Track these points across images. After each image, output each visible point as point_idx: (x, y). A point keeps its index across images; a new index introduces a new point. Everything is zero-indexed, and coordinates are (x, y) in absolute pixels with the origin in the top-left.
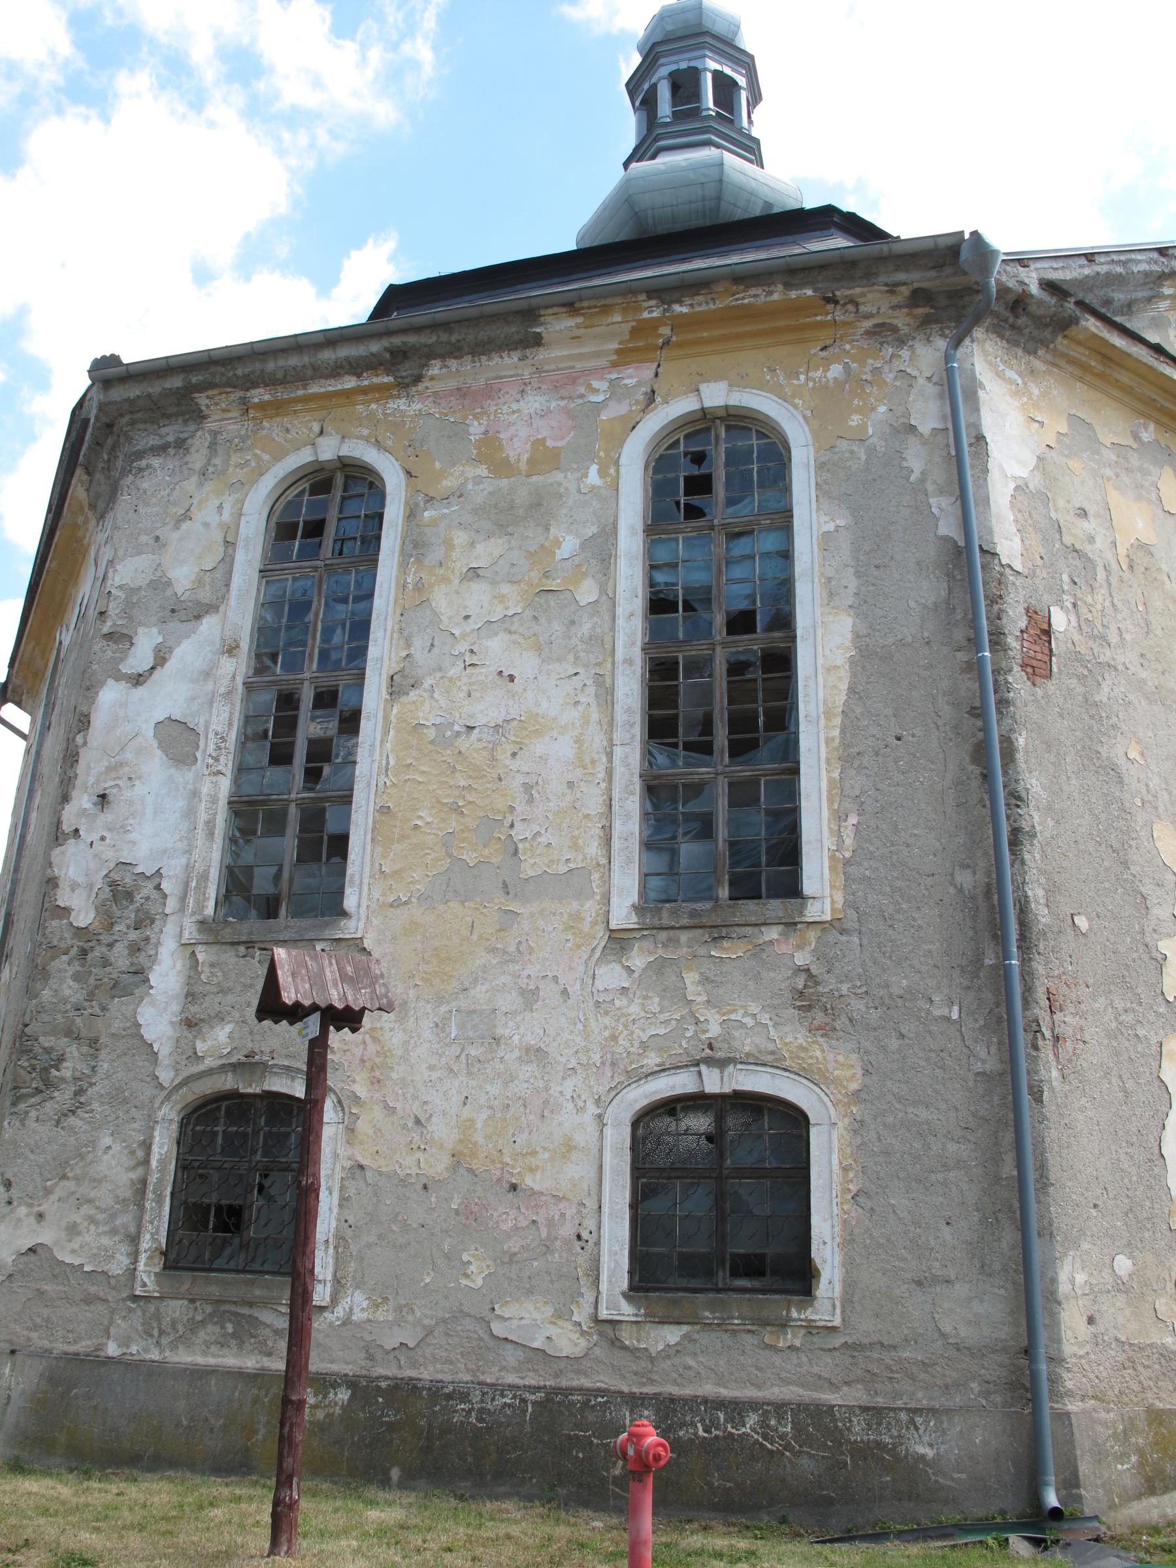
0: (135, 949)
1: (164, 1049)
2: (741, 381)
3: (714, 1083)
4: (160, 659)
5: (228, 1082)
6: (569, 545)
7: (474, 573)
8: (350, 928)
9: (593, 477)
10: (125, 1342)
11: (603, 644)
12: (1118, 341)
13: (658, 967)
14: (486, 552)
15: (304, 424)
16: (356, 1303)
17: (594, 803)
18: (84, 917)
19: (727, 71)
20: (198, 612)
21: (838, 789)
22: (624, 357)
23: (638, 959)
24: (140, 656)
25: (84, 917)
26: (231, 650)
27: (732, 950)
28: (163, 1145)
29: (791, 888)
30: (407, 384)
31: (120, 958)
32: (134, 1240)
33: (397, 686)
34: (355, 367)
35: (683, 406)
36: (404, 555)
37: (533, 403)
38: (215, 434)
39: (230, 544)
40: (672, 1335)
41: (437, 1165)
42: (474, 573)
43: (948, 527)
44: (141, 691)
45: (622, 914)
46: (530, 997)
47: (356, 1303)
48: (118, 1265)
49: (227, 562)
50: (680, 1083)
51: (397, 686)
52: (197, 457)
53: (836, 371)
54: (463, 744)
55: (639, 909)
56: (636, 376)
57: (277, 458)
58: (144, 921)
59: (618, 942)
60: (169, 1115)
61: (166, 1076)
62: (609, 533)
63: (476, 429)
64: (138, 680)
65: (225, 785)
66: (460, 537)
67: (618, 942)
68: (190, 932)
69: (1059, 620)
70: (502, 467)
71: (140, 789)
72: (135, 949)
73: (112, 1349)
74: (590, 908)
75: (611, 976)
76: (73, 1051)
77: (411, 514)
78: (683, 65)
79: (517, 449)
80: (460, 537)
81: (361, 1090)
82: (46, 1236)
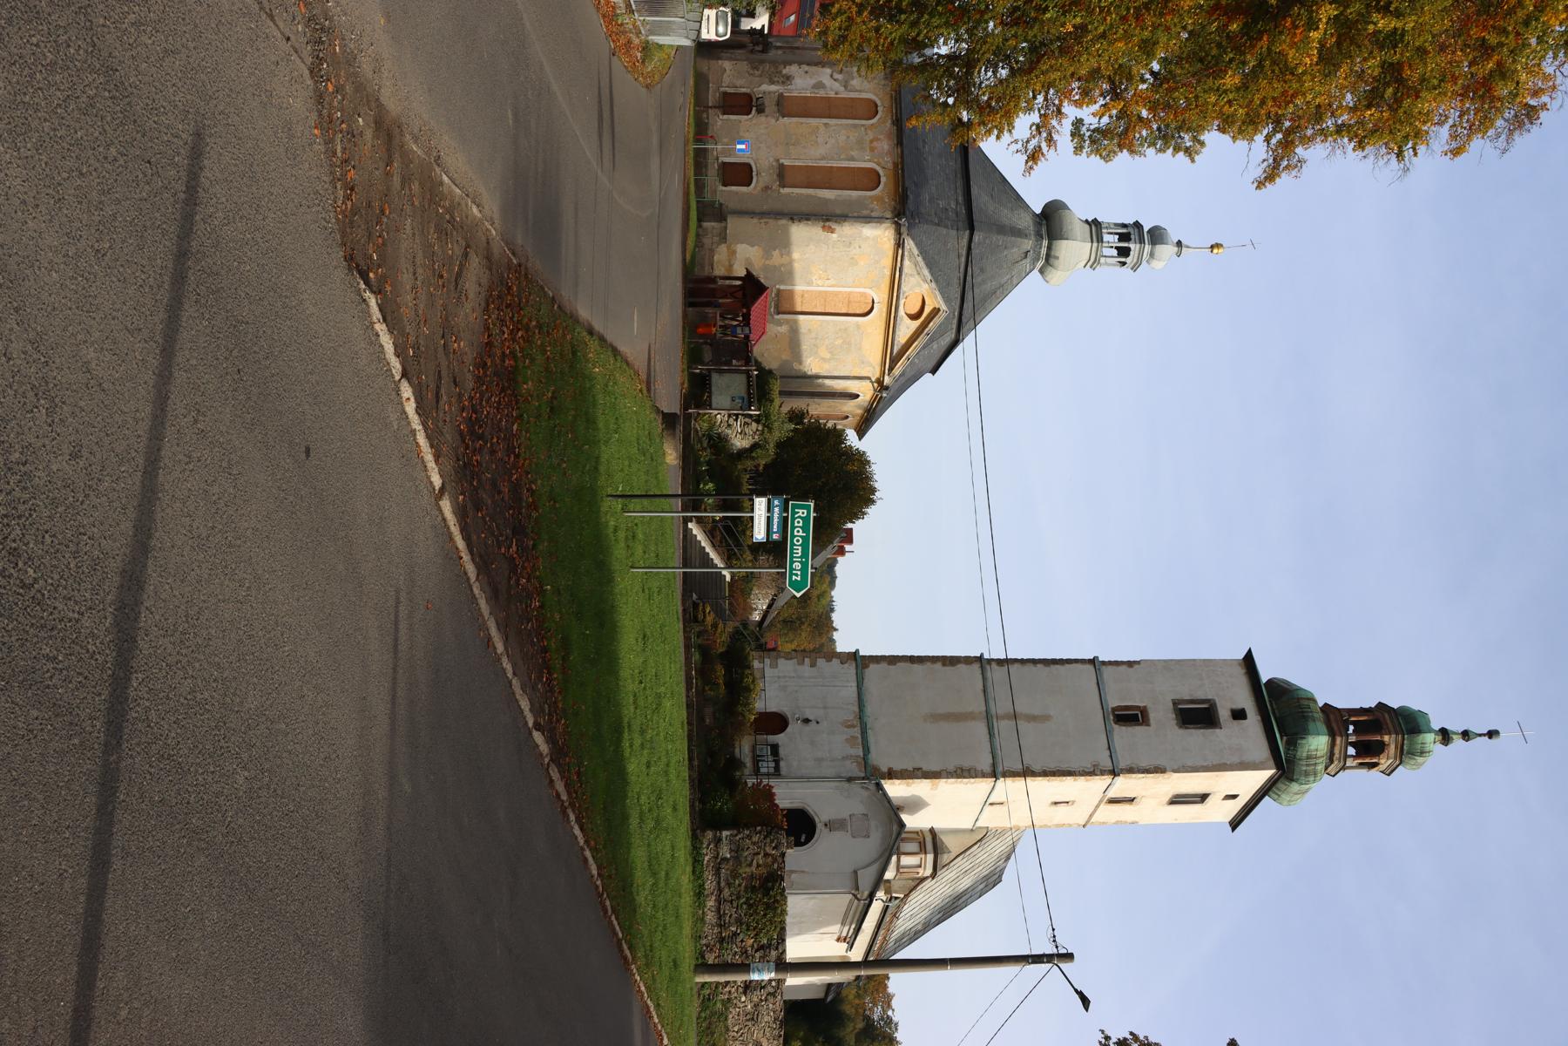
0: (778, 82)
1: (760, 89)
2: (885, 184)
3: (754, 174)
4: (835, 80)
6: (853, 153)
7: (848, 137)
8: (781, 118)
9: (867, 158)
11: (832, 159)
15: (887, 104)
18: (784, 72)
19: (1132, 253)
20: (845, 87)
21: (801, 194)
23: (774, 164)
24: (836, 76)
25: (784, 72)
26: (836, 94)
27: (775, 176)
28: (743, 90)
29: (784, 187)
30: (893, 123)
31: (776, 79)
32: (728, 87)
33: (826, 124)
34: (896, 113)
35: (881, 172)
37: (886, 147)
38: (888, 85)
39: (860, 91)
40: (716, 167)
41: (741, 134)
42: (848, 137)
43: (850, 215)
44: (829, 77)
45: (781, 161)
47: (720, 123)
48: (723, 84)
49: (857, 91)
50: (754, 169)
52: (883, 82)
54: (814, 137)
55: (782, 164)
56: (890, 165)
57: (880, 99)
58: (783, 83)
60: (748, 91)
61: (755, 90)
63: (882, 137)
64: (831, 76)
66: (857, 134)
68: (781, 91)
69: (834, 235)
70: (871, 142)
71: (809, 79)
72: (778, 82)
73: (711, 85)
74: (782, 156)
75: (771, 159)
76: (760, 72)
77: (863, 125)
79: (875, 144)
80: (857, 134)
81: (754, 122)
82: (728, 71)
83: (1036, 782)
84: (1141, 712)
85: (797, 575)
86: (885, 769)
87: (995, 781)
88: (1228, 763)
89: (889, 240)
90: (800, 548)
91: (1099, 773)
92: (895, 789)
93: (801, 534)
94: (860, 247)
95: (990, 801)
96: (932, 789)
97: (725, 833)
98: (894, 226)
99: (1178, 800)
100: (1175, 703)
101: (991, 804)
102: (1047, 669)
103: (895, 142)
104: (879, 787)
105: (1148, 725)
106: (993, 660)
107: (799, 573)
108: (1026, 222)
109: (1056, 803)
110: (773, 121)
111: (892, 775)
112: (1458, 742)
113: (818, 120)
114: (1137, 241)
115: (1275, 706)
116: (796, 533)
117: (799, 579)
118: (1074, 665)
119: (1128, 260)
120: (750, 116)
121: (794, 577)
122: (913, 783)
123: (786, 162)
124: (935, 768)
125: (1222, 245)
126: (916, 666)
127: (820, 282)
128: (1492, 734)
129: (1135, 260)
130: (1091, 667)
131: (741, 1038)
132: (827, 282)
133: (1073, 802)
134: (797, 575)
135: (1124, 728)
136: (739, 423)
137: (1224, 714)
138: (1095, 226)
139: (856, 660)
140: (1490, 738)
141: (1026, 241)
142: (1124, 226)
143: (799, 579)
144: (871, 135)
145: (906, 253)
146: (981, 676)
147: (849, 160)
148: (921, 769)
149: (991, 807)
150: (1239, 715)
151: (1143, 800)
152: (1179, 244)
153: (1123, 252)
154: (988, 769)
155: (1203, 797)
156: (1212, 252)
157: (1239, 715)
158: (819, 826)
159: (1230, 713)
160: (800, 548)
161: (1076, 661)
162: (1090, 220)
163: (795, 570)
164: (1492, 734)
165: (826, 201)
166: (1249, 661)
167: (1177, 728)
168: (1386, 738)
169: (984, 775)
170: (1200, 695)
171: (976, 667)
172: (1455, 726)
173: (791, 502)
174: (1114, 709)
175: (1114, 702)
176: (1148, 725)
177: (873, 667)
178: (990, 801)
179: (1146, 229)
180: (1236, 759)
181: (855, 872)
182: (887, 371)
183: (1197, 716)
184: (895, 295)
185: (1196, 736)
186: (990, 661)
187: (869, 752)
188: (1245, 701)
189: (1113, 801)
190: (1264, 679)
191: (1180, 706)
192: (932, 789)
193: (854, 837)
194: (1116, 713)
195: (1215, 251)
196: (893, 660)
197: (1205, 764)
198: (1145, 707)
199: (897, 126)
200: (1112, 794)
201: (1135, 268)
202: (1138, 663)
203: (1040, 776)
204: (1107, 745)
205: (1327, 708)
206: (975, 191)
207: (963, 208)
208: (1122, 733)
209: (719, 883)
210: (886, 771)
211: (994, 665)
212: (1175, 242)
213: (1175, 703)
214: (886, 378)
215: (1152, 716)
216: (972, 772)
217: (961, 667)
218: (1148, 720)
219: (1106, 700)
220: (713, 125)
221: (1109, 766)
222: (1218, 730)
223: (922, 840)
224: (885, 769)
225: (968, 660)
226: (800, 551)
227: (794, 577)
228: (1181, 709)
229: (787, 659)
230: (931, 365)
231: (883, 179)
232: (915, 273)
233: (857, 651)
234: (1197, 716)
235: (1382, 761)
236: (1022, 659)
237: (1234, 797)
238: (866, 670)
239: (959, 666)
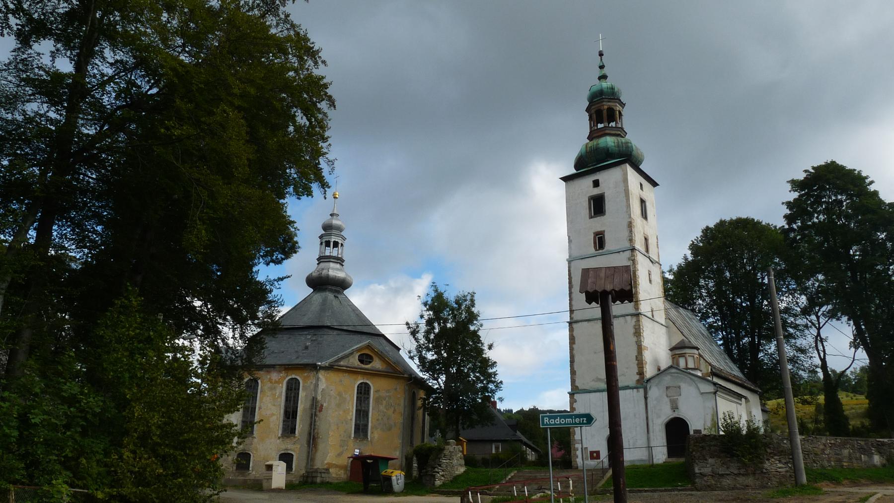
2: (296, 375)
5: (242, 451)
7: (268, 396)
8: (254, 436)
10: (232, 477)
11: (280, 405)
12: (339, 368)
13: (282, 441)
14: (269, 393)
16: (254, 473)
17: (278, 423)
19: (336, 240)
22: (284, 370)
23: (281, 440)
29: (295, 433)
30: (261, 370)
33: (260, 408)
36: (261, 392)
45: (280, 435)
46: (271, 443)
47: (254, 473)
50: (283, 452)
51: (260, 408)
53: (306, 374)
59: (279, 438)
62: (282, 392)
65: (241, 419)
67: (279, 438)
69: (325, 405)
70: (271, 382)
77: (261, 388)
78: (327, 240)
83: (641, 292)
84: (597, 235)
85: (583, 420)
86: (637, 377)
87: (641, 314)
88: (624, 188)
89: (328, 373)
90: (567, 420)
91: (633, 258)
92: (649, 372)
93: (558, 420)
94: (332, 390)
95: (651, 317)
96: (647, 350)
97: (697, 471)
98: (321, 371)
99: (644, 215)
100: (591, 217)
101: (653, 316)
102: (574, 286)
103: (272, 369)
104: (649, 380)
105: (604, 231)
106: (570, 316)
107: (581, 419)
108: (318, 297)
109: (650, 281)
110: (255, 440)
111: (641, 373)
112: (605, 71)
113: (256, 414)
114: (330, 237)
115: (590, 165)
116: (559, 422)
117: (585, 419)
118: (572, 272)
119: (340, 242)
120: (252, 454)
121: (585, 422)
122: (645, 360)
123: (280, 432)
124: (635, 348)
125: (334, 193)
126: (576, 359)
127: (351, 414)
128: (601, 54)
129: (340, 238)
130: (573, 263)
131: (821, 462)
132: (351, 409)
133: (649, 271)
134: (583, 420)
135: (606, 245)
136: (444, 461)
137: (596, 191)
138: (322, 259)
139: (574, 394)
140: (603, 55)
141: (329, 297)
142: (321, 244)
143: (585, 419)
144: (269, 385)
145: (336, 364)
146: (580, 323)
147: (281, 395)
148: (636, 356)
149: (655, 317)
150: (596, 184)
151: (645, 233)
152: (332, 215)
153: (336, 244)
154: (634, 319)
155: (643, 202)
156: (337, 198)
157: (596, 184)
158: (675, 415)
159: (596, 188)
160: (567, 420)
161: (569, 271)
162: (317, 262)
163: (580, 421)
164: (601, 54)
165: (304, 410)
166: (566, 179)
167: (605, 216)
168: (606, 107)
169: (638, 321)
170: (586, 204)
171: (575, 326)
172: (598, 73)
173: (541, 427)
174: (596, 250)
175: (592, 250)
176: (604, 231)
177: (577, 384)
178: (651, 317)
179: (324, 232)
180: (622, 185)
181: (702, 394)
182: (401, 375)
183: (598, 205)
184: (359, 370)
185: (609, 205)
186: (571, 318)
187: (628, 386)
188: (588, 181)
189: (647, 251)
190: (574, 171)
191: (593, 214)
192: (647, 350)
193: (680, 395)
194: (598, 249)
195: (337, 196)
196: (573, 373)
197: (625, 201)
198: (594, 233)
199: (263, 368)
200: (643, 250)
201: (344, 239)
202: (569, 237)
203: (637, 289)
204: (617, 254)
205: (590, 138)
206: (301, 324)
207: (311, 331)
208: (609, 245)
209: (727, 475)
210: (639, 376)
211: (572, 316)
212: (331, 217)
213: (591, 217)
214: (405, 376)
215: (599, 229)
216: (637, 327)
217: (575, 334)
218: (601, 231)
219: (591, 255)
220: (255, 477)
221: (628, 253)
222: (606, 195)
223: (677, 356)
224: (637, 377)
225: (571, 330)
226: (569, 420)
227: (585, 422)
228: (594, 214)
229: (575, 434)
230: (395, 350)
231: (293, 376)
232: (347, 359)
233: (568, 393)
234: (598, 205)
235: (618, 109)
236: (569, 300)
237: (641, 185)
238: (580, 388)
239: (575, 335)
